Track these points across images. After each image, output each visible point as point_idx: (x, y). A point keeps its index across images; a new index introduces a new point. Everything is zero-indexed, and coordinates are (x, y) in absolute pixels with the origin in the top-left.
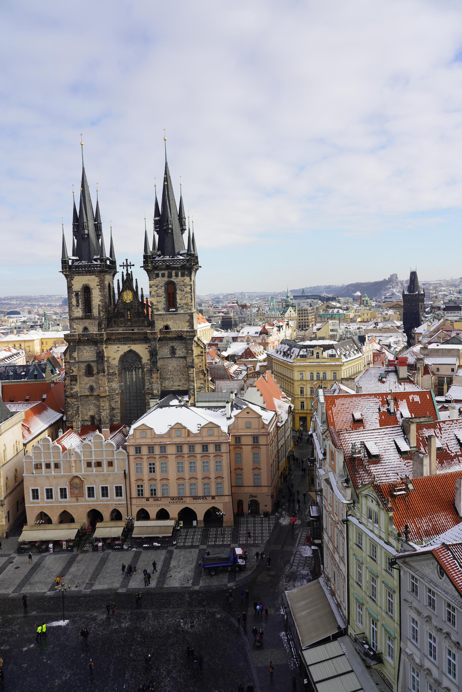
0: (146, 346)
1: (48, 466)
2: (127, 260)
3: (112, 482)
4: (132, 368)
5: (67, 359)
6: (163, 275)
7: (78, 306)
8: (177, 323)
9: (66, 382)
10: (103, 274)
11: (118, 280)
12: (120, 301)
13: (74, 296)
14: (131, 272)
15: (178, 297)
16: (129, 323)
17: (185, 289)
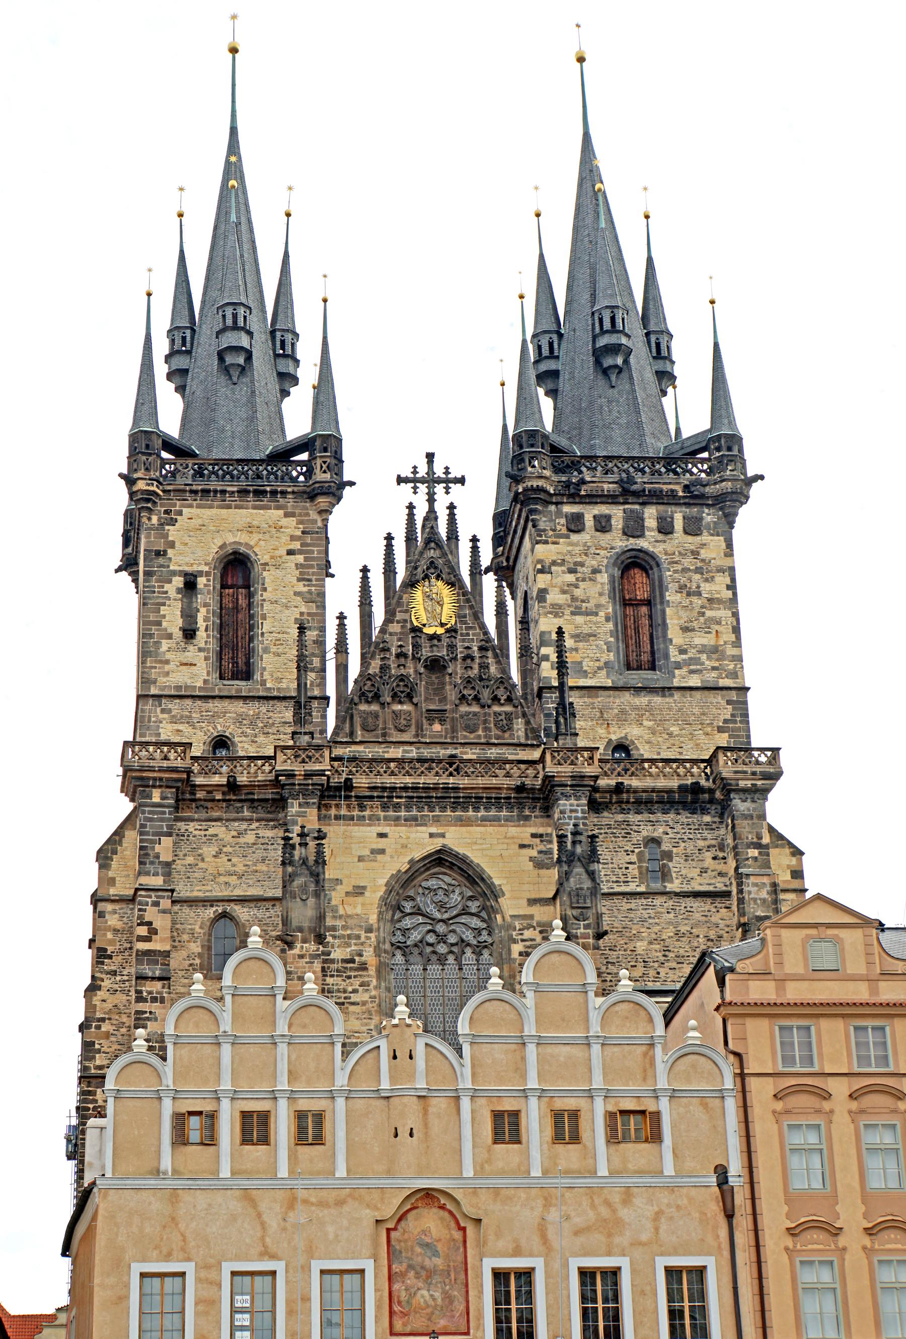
0: (524, 833)
1: (255, 1128)
2: (430, 457)
3: (644, 1237)
4: (442, 949)
5: (112, 882)
6: (603, 524)
7: (189, 634)
8: (670, 735)
9: (96, 1000)
10: (322, 501)
11: (389, 538)
12: (395, 628)
13: (172, 593)
14: (452, 507)
15: (673, 620)
16: (437, 727)
17: (705, 587)
